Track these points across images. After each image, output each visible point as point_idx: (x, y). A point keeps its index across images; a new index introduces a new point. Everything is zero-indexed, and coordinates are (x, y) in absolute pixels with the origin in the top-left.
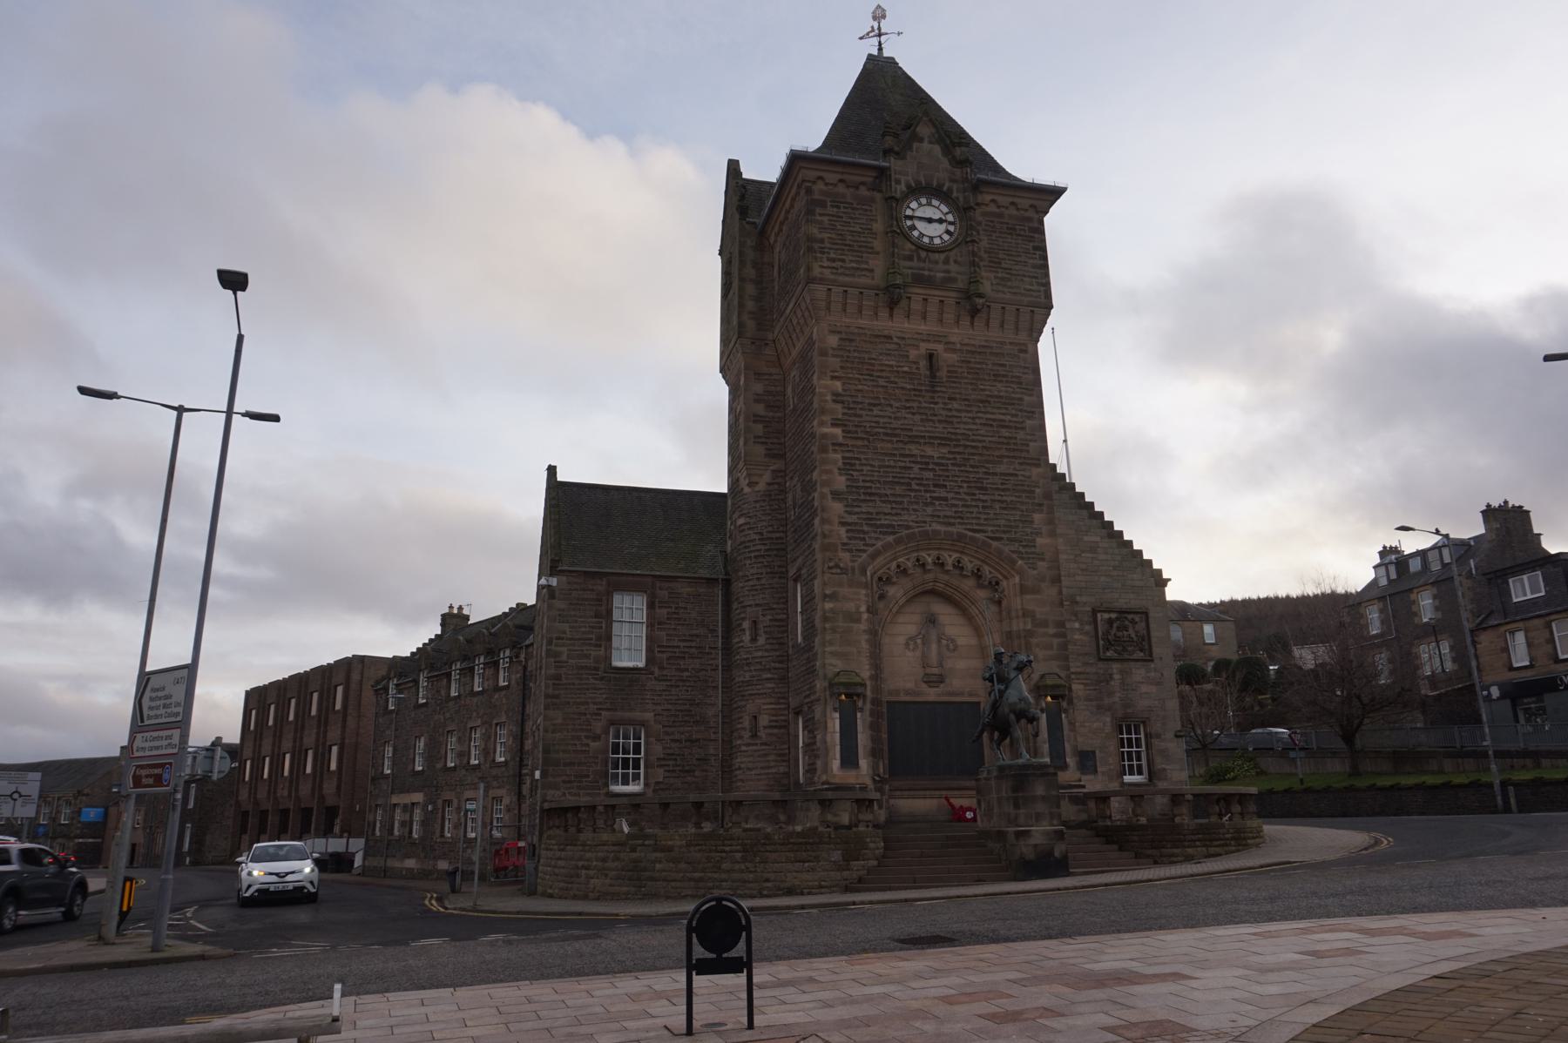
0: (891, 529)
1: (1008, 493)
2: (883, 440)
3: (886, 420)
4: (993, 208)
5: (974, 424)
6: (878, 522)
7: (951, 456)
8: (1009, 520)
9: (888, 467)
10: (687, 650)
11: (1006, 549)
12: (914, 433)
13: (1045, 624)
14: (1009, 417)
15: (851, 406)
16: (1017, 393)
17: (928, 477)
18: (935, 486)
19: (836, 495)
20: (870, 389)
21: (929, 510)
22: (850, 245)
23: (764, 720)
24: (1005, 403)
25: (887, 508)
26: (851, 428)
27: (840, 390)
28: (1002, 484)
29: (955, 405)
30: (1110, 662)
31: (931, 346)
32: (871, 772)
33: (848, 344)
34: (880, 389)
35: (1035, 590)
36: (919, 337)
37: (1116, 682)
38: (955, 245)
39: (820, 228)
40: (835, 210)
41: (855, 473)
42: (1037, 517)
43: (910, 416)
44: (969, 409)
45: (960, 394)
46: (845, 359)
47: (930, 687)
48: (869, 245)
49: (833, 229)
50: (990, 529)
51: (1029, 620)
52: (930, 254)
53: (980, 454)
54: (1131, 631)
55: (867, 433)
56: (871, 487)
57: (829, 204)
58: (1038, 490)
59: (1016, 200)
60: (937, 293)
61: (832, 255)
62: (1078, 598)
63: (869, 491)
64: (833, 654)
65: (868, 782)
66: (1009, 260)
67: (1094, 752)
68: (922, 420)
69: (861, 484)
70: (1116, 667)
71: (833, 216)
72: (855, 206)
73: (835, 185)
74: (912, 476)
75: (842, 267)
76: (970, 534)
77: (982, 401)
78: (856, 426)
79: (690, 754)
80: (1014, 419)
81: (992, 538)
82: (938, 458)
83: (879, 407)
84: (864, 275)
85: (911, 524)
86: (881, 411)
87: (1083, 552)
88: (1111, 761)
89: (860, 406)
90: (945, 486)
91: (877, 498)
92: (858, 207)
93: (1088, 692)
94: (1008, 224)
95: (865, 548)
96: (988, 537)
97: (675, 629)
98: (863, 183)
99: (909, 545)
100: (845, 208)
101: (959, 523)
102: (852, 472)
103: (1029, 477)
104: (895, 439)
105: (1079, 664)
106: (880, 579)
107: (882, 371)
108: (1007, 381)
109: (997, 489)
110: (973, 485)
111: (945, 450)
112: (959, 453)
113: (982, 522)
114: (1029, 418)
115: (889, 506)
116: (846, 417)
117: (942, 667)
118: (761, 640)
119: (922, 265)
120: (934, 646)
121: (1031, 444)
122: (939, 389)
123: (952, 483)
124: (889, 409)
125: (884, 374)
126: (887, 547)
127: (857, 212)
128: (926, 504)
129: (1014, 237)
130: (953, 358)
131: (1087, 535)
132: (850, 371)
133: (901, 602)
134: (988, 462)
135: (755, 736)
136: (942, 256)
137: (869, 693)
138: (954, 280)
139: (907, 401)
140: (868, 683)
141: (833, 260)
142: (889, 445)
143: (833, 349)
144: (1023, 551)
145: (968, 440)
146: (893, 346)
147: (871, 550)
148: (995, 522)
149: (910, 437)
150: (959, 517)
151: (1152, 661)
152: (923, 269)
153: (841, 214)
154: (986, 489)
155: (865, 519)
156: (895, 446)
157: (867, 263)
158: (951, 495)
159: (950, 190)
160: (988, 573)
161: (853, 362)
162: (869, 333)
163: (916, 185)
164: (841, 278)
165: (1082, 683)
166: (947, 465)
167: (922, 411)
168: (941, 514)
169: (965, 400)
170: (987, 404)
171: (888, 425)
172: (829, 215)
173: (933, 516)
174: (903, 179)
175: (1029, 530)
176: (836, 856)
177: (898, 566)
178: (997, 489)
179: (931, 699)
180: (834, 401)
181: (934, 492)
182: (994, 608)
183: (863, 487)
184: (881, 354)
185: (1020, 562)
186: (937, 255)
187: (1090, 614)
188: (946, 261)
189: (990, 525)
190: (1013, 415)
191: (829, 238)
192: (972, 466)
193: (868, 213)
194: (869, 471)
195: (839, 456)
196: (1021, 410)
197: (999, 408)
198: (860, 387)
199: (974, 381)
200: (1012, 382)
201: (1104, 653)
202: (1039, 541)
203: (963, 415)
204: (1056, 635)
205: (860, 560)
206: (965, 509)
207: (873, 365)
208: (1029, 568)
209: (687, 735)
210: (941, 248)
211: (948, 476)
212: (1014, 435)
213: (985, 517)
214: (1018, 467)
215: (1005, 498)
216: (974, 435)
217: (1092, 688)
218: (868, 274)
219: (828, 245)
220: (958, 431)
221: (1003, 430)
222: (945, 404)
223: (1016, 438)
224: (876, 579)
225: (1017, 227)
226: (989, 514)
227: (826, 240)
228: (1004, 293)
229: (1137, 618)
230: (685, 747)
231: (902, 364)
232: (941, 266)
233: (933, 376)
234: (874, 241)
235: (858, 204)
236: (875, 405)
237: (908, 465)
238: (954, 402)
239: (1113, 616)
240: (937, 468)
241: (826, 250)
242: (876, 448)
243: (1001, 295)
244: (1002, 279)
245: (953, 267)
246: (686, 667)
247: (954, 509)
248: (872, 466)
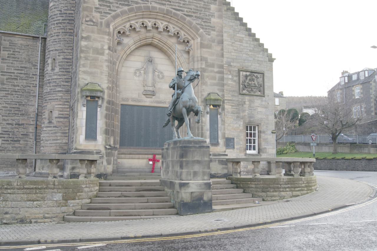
8: (197, 6)
10: (18, 75)
11: (194, 22)
13: (212, 66)
23: (56, 114)
30: (244, 96)
32: (104, 143)
35: (209, 47)
37: (246, 106)
47: (147, 97)
50: (186, 10)
51: (204, 62)
54: (256, 82)
62: (232, 64)
64: (84, 72)
67: (234, 139)
70: (247, 98)
76: (174, 11)
79: (17, 132)
81: (187, 15)
93: (233, 109)
95: (110, 12)
96: (184, 14)
97: (12, 63)
99: (137, 14)
101: (168, 4)
105: (230, 96)
106: (119, 32)
113: (181, 5)
118: (57, 70)
120: (150, 75)
126: (123, 13)
131: (238, 33)
135: (50, 122)
137: (106, 97)
140: (106, 91)
144: (204, 24)
148: (190, 7)
151: (264, 96)
165: (231, 105)
176: (58, 197)
177: (131, 26)
179: (147, 104)
182: (185, 56)
185: (201, 30)
187: (237, 72)
189: (186, 8)
201: (242, 91)
205: (106, 18)
209: (16, 121)
217: (235, 107)
224: (116, 32)
229: (259, 75)
230: (15, 128)
239: (248, 74)
246: (18, 84)
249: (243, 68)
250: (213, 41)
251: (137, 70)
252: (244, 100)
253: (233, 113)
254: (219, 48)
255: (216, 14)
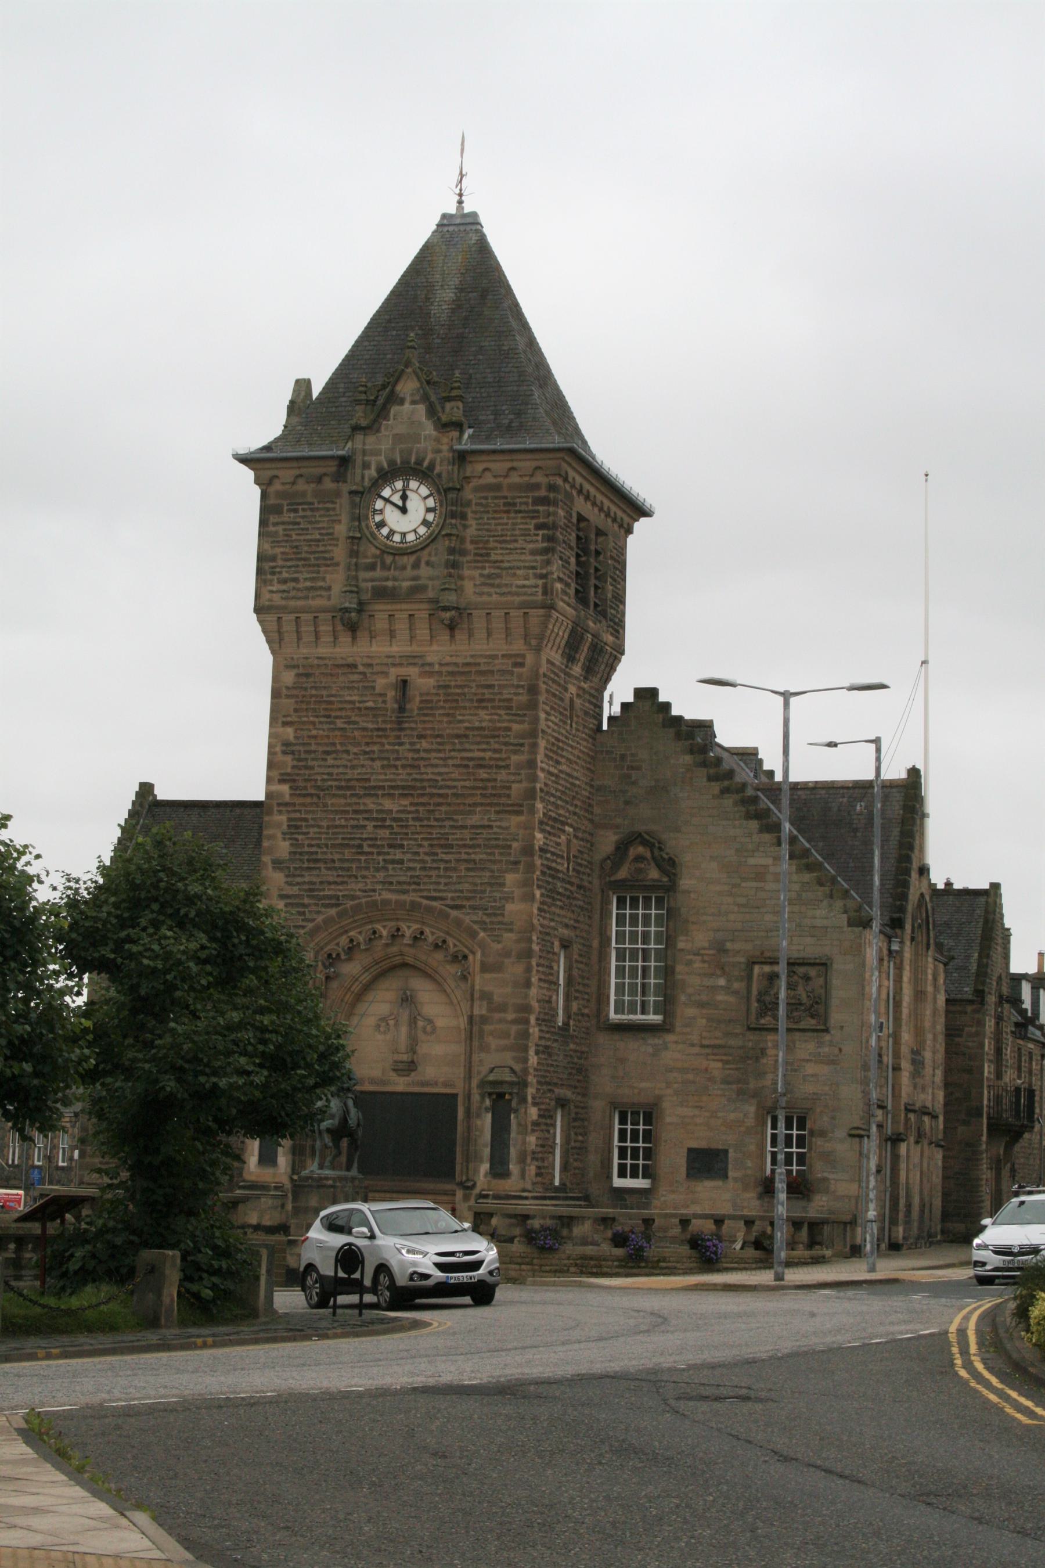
0: (335, 901)
1: (477, 850)
2: (334, 795)
3: (341, 770)
4: (489, 479)
5: (445, 766)
6: (322, 893)
7: (413, 809)
8: (476, 885)
9: (336, 827)
11: (467, 919)
12: (372, 784)
13: (502, 1008)
14: (489, 754)
15: (303, 756)
16: (504, 721)
17: (383, 835)
18: (390, 846)
19: (278, 864)
20: (326, 733)
21: (381, 876)
22: (305, 559)
24: (487, 737)
25: (331, 876)
26: (301, 784)
27: (291, 738)
28: (471, 839)
29: (425, 744)
30: (764, 1033)
31: (403, 671)
32: (289, 1170)
33: (305, 680)
34: (337, 733)
35: (497, 968)
36: (390, 661)
38: (432, 540)
39: (273, 542)
40: (292, 515)
41: (300, 837)
42: (510, 878)
43: (369, 763)
44: (441, 747)
45: (433, 729)
46: (300, 699)
47: (399, 1075)
48: (327, 555)
49: (287, 541)
50: (450, 895)
51: (485, 1003)
52: (397, 557)
53: (449, 805)
55: (318, 788)
56: (317, 853)
57: (285, 508)
58: (515, 845)
59: (515, 464)
60: (404, 606)
61: (285, 575)
62: (729, 945)
63: (314, 857)
65: (285, 1181)
66: (502, 548)
67: (726, 1152)
68: (383, 767)
69: (306, 849)
71: (289, 523)
72: (316, 506)
73: (293, 483)
74: (365, 836)
75: (294, 588)
76: (425, 902)
77: (458, 736)
78: (306, 780)
80: (497, 756)
81: (453, 907)
82: (398, 812)
83: (334, 756)
84: (317, 596)
85: (358, 893)
86: (336, 759)
87: (744, 879)
88: (749, 1164)
89: (313, 756)
90: (402, 846)
91: (322, 865)
92: (321, 506)
93: (728, 1072)
94: (506, 498)
95: (304, 924)
96: (446, 906)
98: (325, 474)
99: (356, 918)
100: (303, 510)
101: (414, 890)
102: (296, 836)
103: (507, 828)
104: (348, 793)
105: (718, 1034)
106: (330, 956)
107: (341, 709)
108: (493, 707)
109: (465, 846)
110: (435, 842)
111: (405, 802)
112: (423, 804)
113: (442, 887)
114: (515, 752)
115: (335, 874)
116: (297, 771)
117: (415, 1053)
119: (386, 574)
120: (404, 1030)
121: (514, 786)
122: (406, 725)
123: (411, 842)
124: (345, 756)
125: (343, 714)
126: (328, 921)
127: (317, 514)
128: (378, 870)
129: (512, 515)
130: (427, 683)
131: (753, 856)
132: (304, 714)
133: (366, 978)
134: (455, 812)
136: (412, 558)
138: (423, 588)
139: (367, 744)
141: (285, 581)
142: (342, 801)
143: (288, 688)
144: (488, 920)
145: (435, 787)
146: (356, 677)
147: (310, 925)
148: (459, 887)
149: (365, 788)
150: (415, 883)
151: (826, 1030)
152: (387, 579)
153: (298, 520)
154: (451, 846)
155: (306, 890)
156: (349, 801)
157: (324, 579)
158: (409, 856)
159: (432, 466)
160: (451, 946)
161: (309, 703)
162: (330, 663)
163: (402, 463)
164: (292, 603)
165: (721, 1060)
166: (407, 820)
167: (383, 755)
168: (394, 880)
169: (438, 736)
170: (464, 740)
171: (342, 777)
172: (283, 523)
173: (383, 883)
174: (373, 461)
175: (498, 895)
177: (352, 941)
178: (465, 846)
179: (400, 1088)
180: (284, 753)
181: (388, 853)
183: (307, 853)
184: (342, 688)
185: (482, 934)
186: (405, 558)
187: (743, 966)
188: (416, 565)
189: (451, 891)
190: (495, 751)
191: (283, 553)
192: (436, 820)
193: (331, 513)
194: (315, 833)
195: (283, 818)
196: (506, 744)
197: (479, 743)
198: (314, 732)
199: (451, 712)
200: (499, 708)
201: (757, 1019)
202: (509, 907)
203: (434, 755)
204: (515, 1022)
206: (423, 873)
207: (331, 703)
208: (493, 941)
210: (431, 534)
211: (407, 834)
212: (494, 776)
213: (446, 881)
214: (493, 817)
215: (473, 856)
216: (443, 780)
217: (732, 1066)
218: (324, 593)
219: (280, 563)
220: (425, 777)
221: (481, 771)
222: (412, 744)
223: (495, 780)
225: (518, 500)
226: (451, 877)
227: (279, 556)
228: (490, 595)
229: (813, 972)
231: (365, 699)
232: (409, 572)
233: (402, 709)
234: (335, 548)
235: (319, 503)
236: (328, 753)
237: (362, 823)
238: (423, 741)
240: (394, 824)
241: (278, 570)
242: (325, 805)
243: (485, 598)
244: (489, 576)
245: (424, 571)
247: (409, 874)
248: (319, 827)
249: (762, 953)
250: (507, 954)
251: (380, 1020)
252: (761, 1046)
253: (726, 1081)
254: (519, 969)
255: (518, 892)
